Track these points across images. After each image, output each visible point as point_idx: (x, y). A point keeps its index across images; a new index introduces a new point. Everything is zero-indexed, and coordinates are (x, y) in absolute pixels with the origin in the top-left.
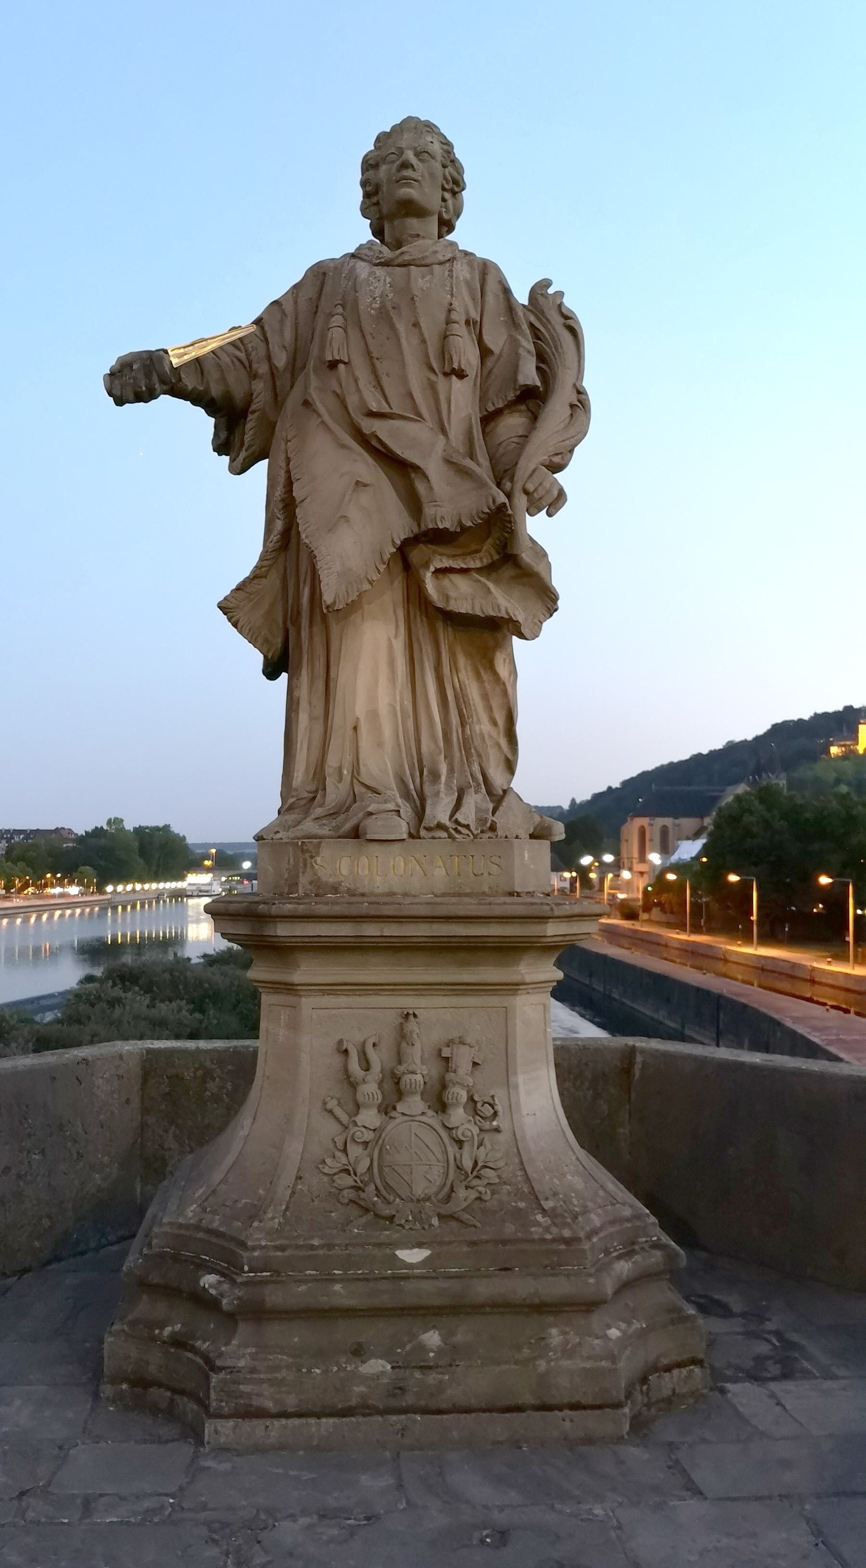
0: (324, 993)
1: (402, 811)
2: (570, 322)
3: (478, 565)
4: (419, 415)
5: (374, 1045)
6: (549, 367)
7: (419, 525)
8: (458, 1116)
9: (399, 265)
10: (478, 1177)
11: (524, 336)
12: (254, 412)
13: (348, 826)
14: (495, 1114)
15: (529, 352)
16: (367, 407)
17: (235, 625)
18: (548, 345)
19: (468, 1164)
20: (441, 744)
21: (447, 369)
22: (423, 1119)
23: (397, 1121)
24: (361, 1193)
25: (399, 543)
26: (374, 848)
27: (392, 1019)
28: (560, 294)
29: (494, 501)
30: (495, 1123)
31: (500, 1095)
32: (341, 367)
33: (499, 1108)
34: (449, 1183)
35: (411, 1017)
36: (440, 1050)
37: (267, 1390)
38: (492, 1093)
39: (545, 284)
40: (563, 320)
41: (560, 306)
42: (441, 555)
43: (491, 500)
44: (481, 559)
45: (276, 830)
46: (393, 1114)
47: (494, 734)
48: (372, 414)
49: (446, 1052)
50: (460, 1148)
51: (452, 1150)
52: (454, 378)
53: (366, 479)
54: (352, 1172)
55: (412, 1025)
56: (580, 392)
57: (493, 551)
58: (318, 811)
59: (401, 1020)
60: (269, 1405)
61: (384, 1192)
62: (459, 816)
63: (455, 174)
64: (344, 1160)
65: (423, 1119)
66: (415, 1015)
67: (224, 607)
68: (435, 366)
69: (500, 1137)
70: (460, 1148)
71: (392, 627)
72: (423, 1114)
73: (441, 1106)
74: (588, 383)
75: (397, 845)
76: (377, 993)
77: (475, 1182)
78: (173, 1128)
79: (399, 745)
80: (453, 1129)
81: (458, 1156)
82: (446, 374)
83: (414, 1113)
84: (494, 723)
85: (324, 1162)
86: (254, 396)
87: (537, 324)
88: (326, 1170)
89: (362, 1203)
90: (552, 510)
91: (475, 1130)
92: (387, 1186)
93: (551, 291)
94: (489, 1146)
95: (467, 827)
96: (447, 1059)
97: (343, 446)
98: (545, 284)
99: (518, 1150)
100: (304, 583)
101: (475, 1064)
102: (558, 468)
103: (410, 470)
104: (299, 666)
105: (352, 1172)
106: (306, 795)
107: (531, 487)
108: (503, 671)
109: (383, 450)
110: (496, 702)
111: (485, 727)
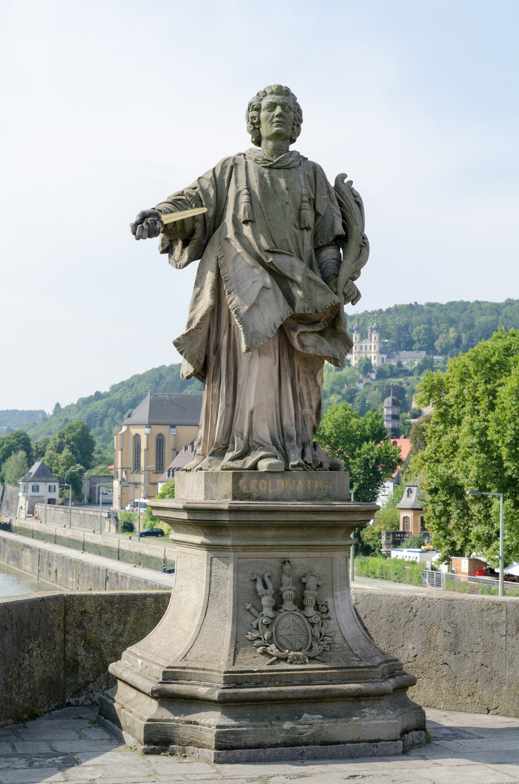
1: (278, 456)
2: (358, 200)
4: (290, 251)
5: (269, 577)
6: (347, 222)
7: (294, 310)
8: (310, 611)
9: (276, 168)
10: (322, 640)
11: (335, 205)
14: (328, 611)
15: (339, 216)
17: (181, 353)
18: (347, 210)
19: (318, 635)
20: (294, 420)
22: (296, 613)
23: (283, 614)
26: (268, 475)
27: (276, 563)
28: (351, 182)
31: (330, 601)
33: (329, 607)
34: (310, 643)
35: (287, 562)
36: (301, 579)
38: (326, 600)
39: (344, 176)
40: (352, 197)
41: (352, 190)
42: (302, 324)
46: (281, 610)
49: (304, 580)
50: (313, 627)
52: (305, 230)
54: (263, 639)
55: (287, 567)
56: (364, 238)
57: (326, 323)
59: (281, 564)
62: (306, 459)
63: (299, 116)
65: (296, 613)
66: (289, 562)
67: (177, 344)
68: (297, 225)
69: (331, 622)
70: (313, 627)
71: (273, 360)
72: (295, 610)
73: (302, 607)
74: (367, 232)
75: (280, 474)
77: (322, 643)
79: (273, 421)
81: (313, 630)
82: (301, 229)
84: (311, 408)
86: (196, 231)
87: (340, 199)
90: (354, 302)
91: (319, 619)
92: (281, 645)
93: (346, 181)
94: (326, 627)
95: (310, 465)
98: (344, 176)
100: (224, 333)
101: (318, 586)
103: (288, 280)
104: (217, 376)
105: (263, 639)
106: (221, 446)
107: (346, 291)
108: (319, 381)
110: (314, 396)
111: (307, 410)
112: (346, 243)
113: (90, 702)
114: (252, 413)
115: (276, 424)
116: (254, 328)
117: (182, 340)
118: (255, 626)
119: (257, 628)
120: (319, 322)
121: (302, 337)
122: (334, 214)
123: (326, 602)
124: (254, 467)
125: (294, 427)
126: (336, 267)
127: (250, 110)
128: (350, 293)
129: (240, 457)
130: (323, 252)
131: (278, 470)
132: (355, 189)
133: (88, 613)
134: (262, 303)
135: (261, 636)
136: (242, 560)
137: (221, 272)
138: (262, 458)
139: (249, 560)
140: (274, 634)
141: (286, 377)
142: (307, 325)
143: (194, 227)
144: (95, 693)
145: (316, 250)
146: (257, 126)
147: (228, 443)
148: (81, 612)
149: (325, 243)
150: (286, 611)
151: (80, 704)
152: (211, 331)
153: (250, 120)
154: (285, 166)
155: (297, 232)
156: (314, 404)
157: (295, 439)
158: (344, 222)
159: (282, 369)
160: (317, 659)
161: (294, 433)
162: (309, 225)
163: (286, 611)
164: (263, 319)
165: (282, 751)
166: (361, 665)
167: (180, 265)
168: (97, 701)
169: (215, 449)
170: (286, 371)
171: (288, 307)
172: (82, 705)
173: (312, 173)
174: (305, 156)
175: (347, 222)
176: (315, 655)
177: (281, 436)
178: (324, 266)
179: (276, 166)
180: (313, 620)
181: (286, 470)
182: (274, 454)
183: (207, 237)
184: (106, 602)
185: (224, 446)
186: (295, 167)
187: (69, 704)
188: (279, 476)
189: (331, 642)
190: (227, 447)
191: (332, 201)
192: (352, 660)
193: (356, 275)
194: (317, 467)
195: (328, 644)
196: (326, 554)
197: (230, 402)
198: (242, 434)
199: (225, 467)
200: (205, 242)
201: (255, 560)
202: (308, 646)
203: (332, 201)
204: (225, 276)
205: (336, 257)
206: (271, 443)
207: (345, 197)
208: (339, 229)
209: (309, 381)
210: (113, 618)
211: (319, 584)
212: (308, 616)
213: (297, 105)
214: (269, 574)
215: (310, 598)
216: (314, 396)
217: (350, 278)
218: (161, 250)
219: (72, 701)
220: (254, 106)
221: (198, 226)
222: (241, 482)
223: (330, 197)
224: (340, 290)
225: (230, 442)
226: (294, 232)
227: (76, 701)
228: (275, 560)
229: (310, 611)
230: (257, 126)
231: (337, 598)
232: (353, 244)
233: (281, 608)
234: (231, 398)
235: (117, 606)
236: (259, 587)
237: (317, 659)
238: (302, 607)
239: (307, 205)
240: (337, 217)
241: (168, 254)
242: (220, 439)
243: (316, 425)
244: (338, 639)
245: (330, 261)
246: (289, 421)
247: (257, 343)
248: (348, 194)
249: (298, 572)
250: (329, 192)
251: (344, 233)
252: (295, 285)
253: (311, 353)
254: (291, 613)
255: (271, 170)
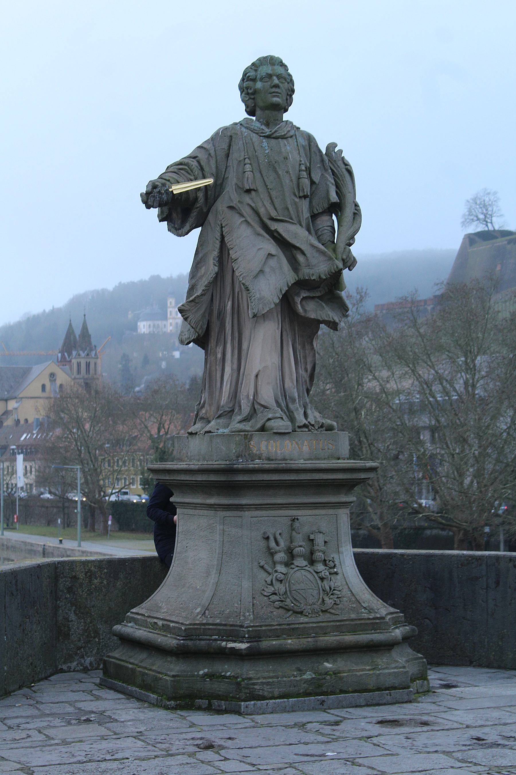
0: (257, 509)
1: (284, 418)
2: (348, 167)
3: (318, 294)
4: (292, 219)
5: (280, 534)
6: (340, 191)
9: (274, 138)
10: (332, 594)
11: (328, 174)
12: (197, 208)
13: (259, 426)
15: (332, 184)
16: (270, 215)
19: (328, 588)
21: (301, 194)
22: (306, 568)
24: (284, 603)
25: (290, 285)
26: (277, 437)
27: (287, 521)
28: (341, 151)
29: (337, 267)
30: (335, 570)
31: (336, 556)
32: (253, 193)
33: (336, 563)
34: (321, 597)
36: (309, 536)
37: (266, 688)
38: (332, 556)
39: (335, 145)
41: (343, 158)
42: (304, 289)
43: (336, 267)
44: (320, 291)
45: (217, 427)
46: (293, 566)
47: (305, 376)
48: (272, 219)
49: (312, 537)
50: (322, 582)
51: (319, 582)
52: (303, 199)
53: (273, 252)
55: (297, 524)
56: (356, 205)
57: (326, 288)
58: (239, 418)
59: (290, 522)
60: (266, 694)
61: (294, 602)
64: (273, 589)
65: (306, 568)
66: (297, 519)
68: (297, 194)
69: (338, 577)
70: (322, 582)
71: (277, 324)
72: (306, 566)
74: (358, 200)
76: (280, 509)
77: (332, 596)
78: (74, 608)
79: (277, 384)
80: (319, 572)
83: (303, 566)
84: (306, 371)
85: (263, 590)
86: (199, 200)
88: (265, 594)
89: (286, 607)
90: (351, 268)
91: (328, 574)
94: (334, 581)
96: (312, 540)
97: (259, 234)
98: (335, 145)
99: (346, 582)
102: (350, 245)
106: (227, 409)
107: (344, 257)
109: (279, 237)
110: (309, 360)
112: (340, 211)
113: (81, 668)
114: (257, 376)
115: (279, 387)
116: (260, 294)
117: (187, 306)
118: (269, 582)
119: (272, 584)
120: (319, 287)
121: (304, 303)
122: (328, 183)
123: (333, 558)
124: (263, 429)
125: (296, 390)
126: (330, 234)
127: (245, 81)
128: (348, 259)
129: (246, 419)
130: (318, 219)
131: (287, 431)
132: (346, 158)
133: (78, 578)
134: (267, 270)
135: (276, 592)
136: (254, 519)
137: (226, 239)
138: (269, 419)
139: (261, 518)
140: (288, 589)
141: (288, 341)
142: (309, 290)
143: (196, 196)
144: (86, 658)
145: (311, 217)
146: (252, 97)
147: (234, 405)
148: (71, 578)
149: (321, 211)
150: (297, 566)
151: (72, 670)
152: (214, 298)
153: (245, 90)
154: (282, 135)
155: (297, 200)
156: (309, 368)
157: (297, 401)
158: (338, 190)
159: (284, 333)
160: (330, 612)
161: (296, 395)
162: (307, 193)
163: (297, 566)
164: (269, 285)
165: (305, 700)
166: (371, 617)
167: (182, 233)
168: (88, 666)
169: (221, 412)
170: (288, 335)
171: (292, 273)
172: (74, 671)
173: (307, 143)
174: (297, 126)
175: (340, 191)
176: (328, 608)
177: (284, 399)
178: (320, 233)
179: (274, 136)
180: (322, 574)
181: (293, 431)
182: (279, 416)
183: (208, 206)
184: (95, 566)
185: (230, 409)
186: (291, 137)
187: (62, 671)
188: (287, 437)
189: (340, 596)
190: (233, 411)
191: (326, 170)
192: (362, 613)
193: (351, 242)
194: (319, 428)
195: (337, 598)
196: (331, 511)
197: (235, 366)
198: (248, 396)
199: (234, 430)
200: (205, 210)
201: (266, 518)
202: (321, 600)
203: (326, 170)
204: (230, 243)
205: (331, 225)
206: (275, 405)
207: (336, 166)
208: (334, 197)
209: (306, 344)
210: (102, 583)
211: (326, 540)
212: (318, 571)
213: (290, 75)
214: (279, 531)
215: (319, 555)
216: (309, 360)
217: (347, 245)
218: (160, 219)
219: (65, 667)
220: (249, 76)
221: (201, 195)
222: (252, 444)
223: (324, 166)
224: (340, 256)
225: (237, 405)
226: (294, 200)
227: (68, 667)
228: (285, 518)
229: (320, 567)
230: (252, 97)
231: (342, 553)
232: (348, 212)
233: (293, 564)
234: (236, 362)
235: (106, 571)
236: (273, 544)
237: (330, 612)
238: (312, 562)
239: (304, 174)
240: (331, 185)
241: (166, 222)
242: (226, 402)
243: (309, 387)
244: (346, 592)
245: (325, 228)
246: (291, 384)
247: (263, 309)
248: (340, 163)
249: (306, 529)
250: (322, 161)
251: (339, 201)
252: (299, 252)
253: (312, 317)
254: (302, 568)
255: (269, 140)
